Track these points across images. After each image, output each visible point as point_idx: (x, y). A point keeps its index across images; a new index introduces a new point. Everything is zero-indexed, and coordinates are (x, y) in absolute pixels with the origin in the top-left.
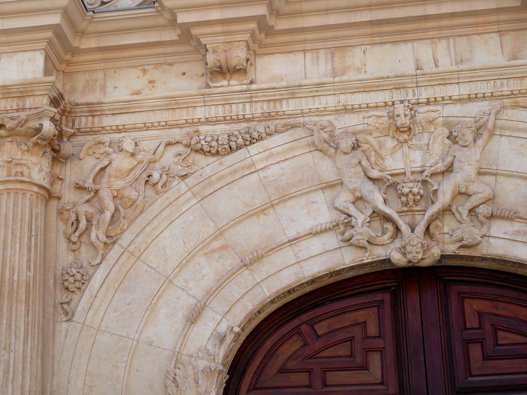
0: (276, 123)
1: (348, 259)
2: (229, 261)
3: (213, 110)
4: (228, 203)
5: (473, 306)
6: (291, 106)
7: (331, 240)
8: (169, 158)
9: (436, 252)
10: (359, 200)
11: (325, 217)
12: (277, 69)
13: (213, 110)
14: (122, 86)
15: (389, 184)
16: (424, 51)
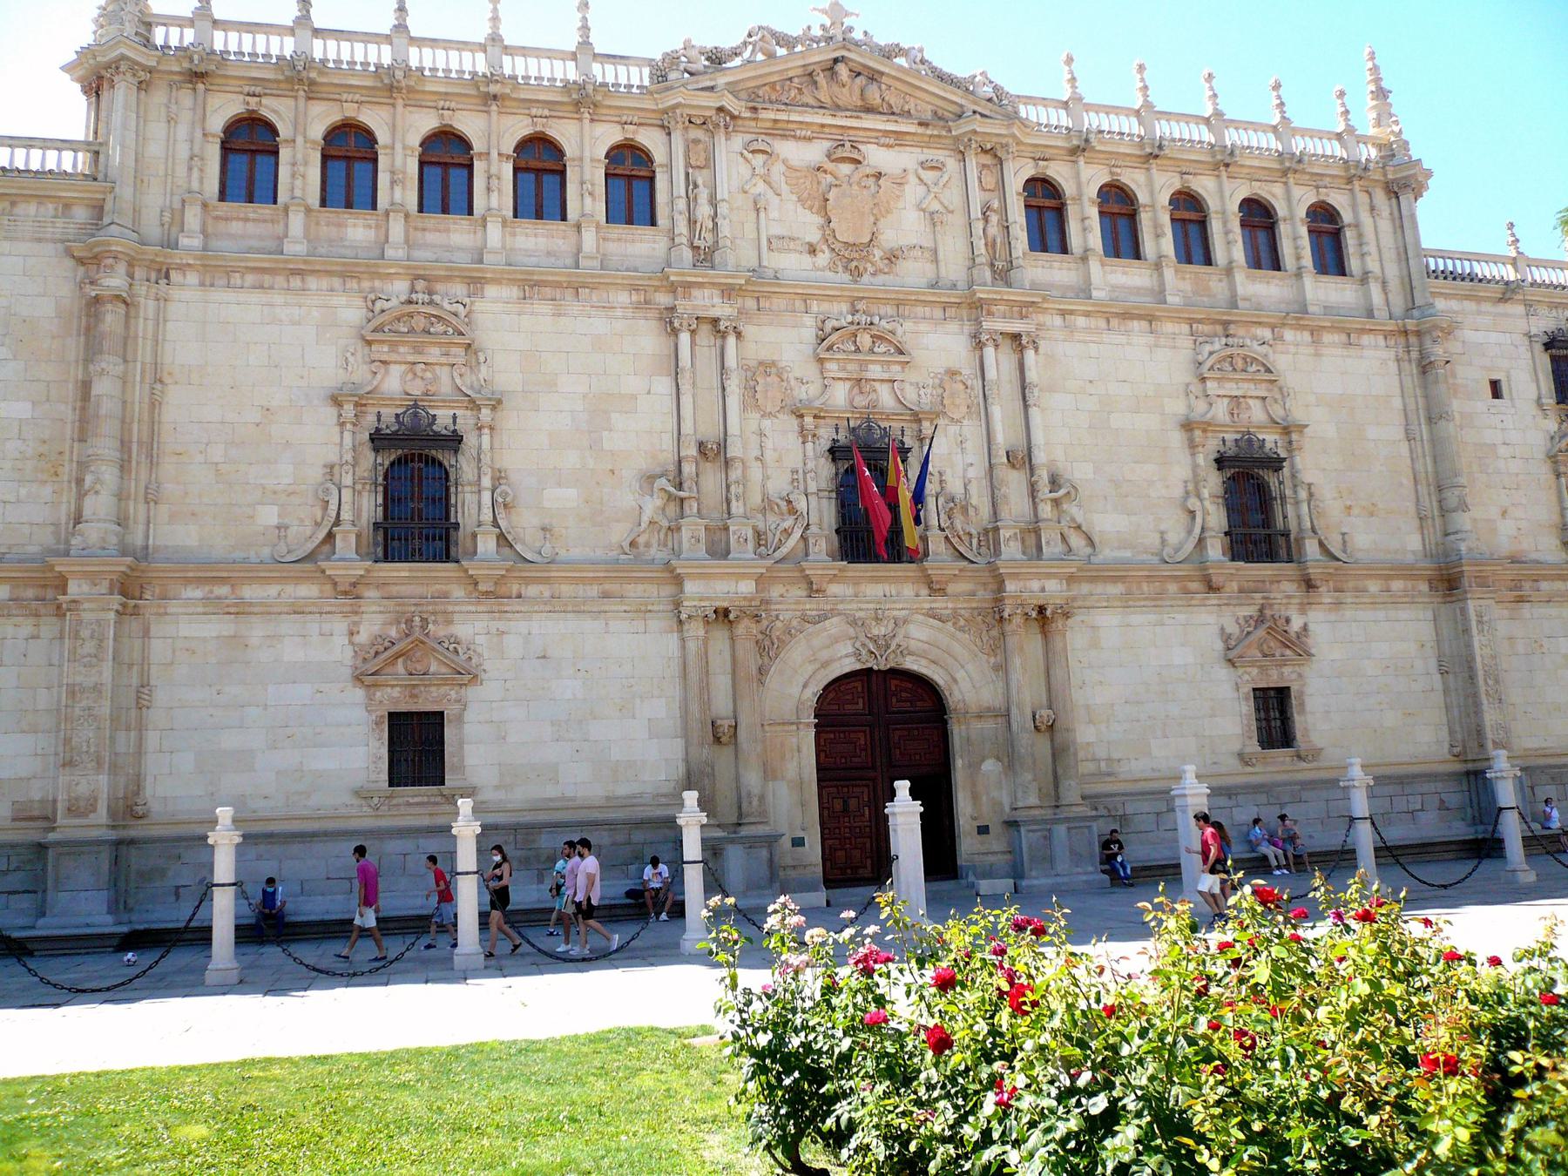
0: (833, 613)
1: (858, 667)
2: (817, 665)
3: (811, 607)
4: (817, 642)
5: (894, 682)
6: (840, 607)
7: (853, 659)
8: (795, 623)
9: (891, 664)
10: (863, 645)
11: (851, 650)
12: (834, 589)
13: (811, 607)
14: (776, 591)
15: (874, 640)
16: (887, 588)
